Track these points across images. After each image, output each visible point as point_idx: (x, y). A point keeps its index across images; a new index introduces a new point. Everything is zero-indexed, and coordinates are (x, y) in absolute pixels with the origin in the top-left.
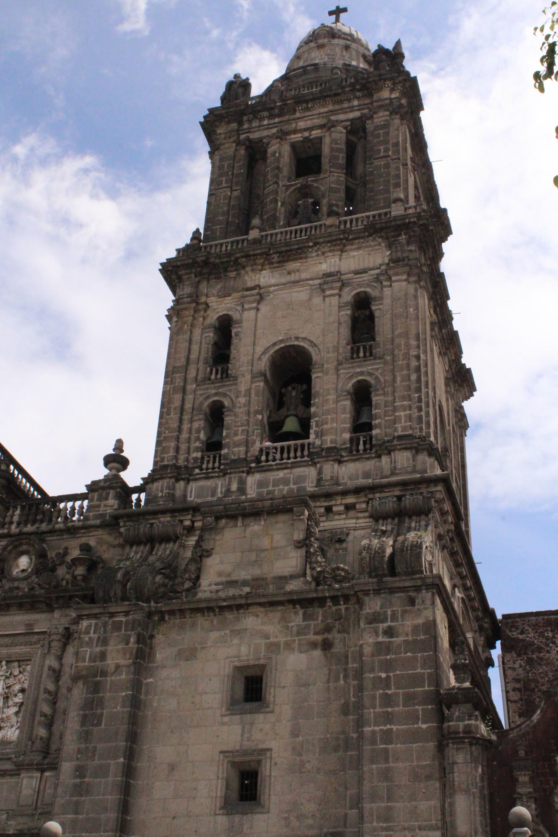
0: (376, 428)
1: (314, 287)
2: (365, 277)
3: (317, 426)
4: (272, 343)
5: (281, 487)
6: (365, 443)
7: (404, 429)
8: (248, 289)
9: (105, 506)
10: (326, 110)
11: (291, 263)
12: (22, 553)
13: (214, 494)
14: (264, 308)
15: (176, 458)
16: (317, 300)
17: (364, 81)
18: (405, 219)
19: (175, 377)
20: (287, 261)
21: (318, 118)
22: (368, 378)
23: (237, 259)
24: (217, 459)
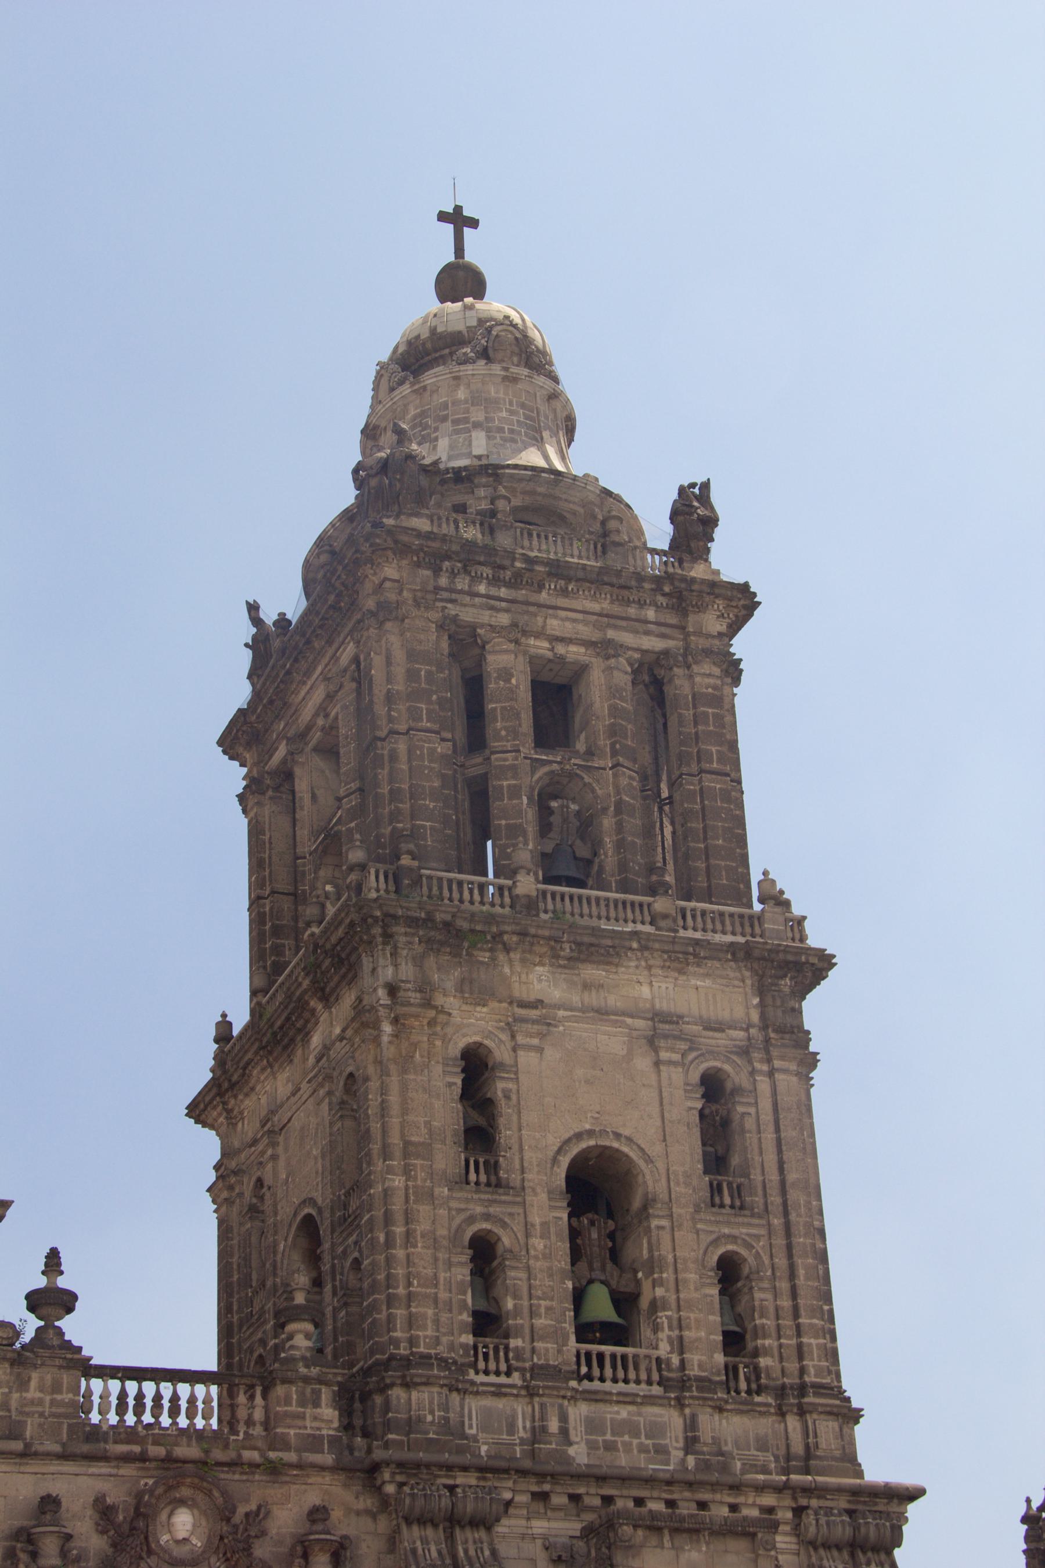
0: (766, 1354)
1: (635, 1034)
2: (720, 1040)
3: (670, 1328)
4: (572, 1133)
5: (626, 1438)
6: (748, 1380)
7: (819, 1372)
8: (523, 1005)
9: (315, 1418)
10: (596, 607)
11: (589, 966)
12: (182, 1502)
13: (511, 1429)
14: (551, 1054)
15: (437, 1341)
16: (643, 1063)
17: (683, 585)
18: (801, 954)
19: (414, 1165)
20: (584, 961)
21: (586, 623)
22: (744, 1252)
23: (501, 934)
24: (502, 1354)
